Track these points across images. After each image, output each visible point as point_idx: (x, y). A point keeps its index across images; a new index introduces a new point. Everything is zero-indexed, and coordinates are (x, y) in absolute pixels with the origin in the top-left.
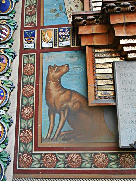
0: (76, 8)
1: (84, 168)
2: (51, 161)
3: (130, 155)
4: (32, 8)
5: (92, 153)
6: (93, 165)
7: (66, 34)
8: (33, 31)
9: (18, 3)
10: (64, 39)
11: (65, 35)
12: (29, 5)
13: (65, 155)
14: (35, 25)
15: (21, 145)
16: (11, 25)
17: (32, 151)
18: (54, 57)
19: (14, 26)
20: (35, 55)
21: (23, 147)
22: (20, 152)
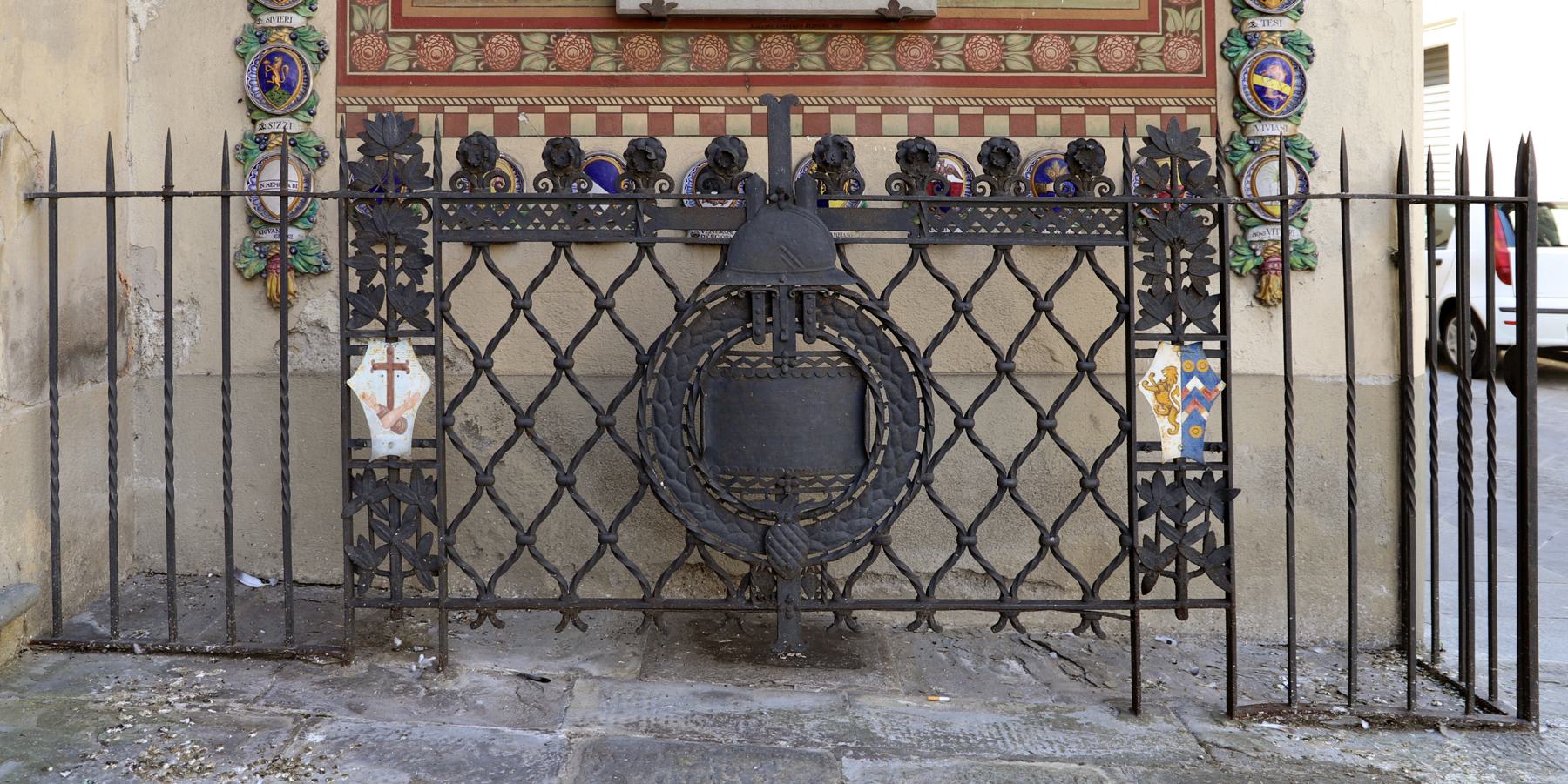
1: (525, 70)
2: (439, 54)
3: (651, 39)
5: (549, 34)
6: (551, 64)
13: (477, 38)
15: (355, 12)
17: (386, 28)
21: (362, 18)
22: (352, 29)
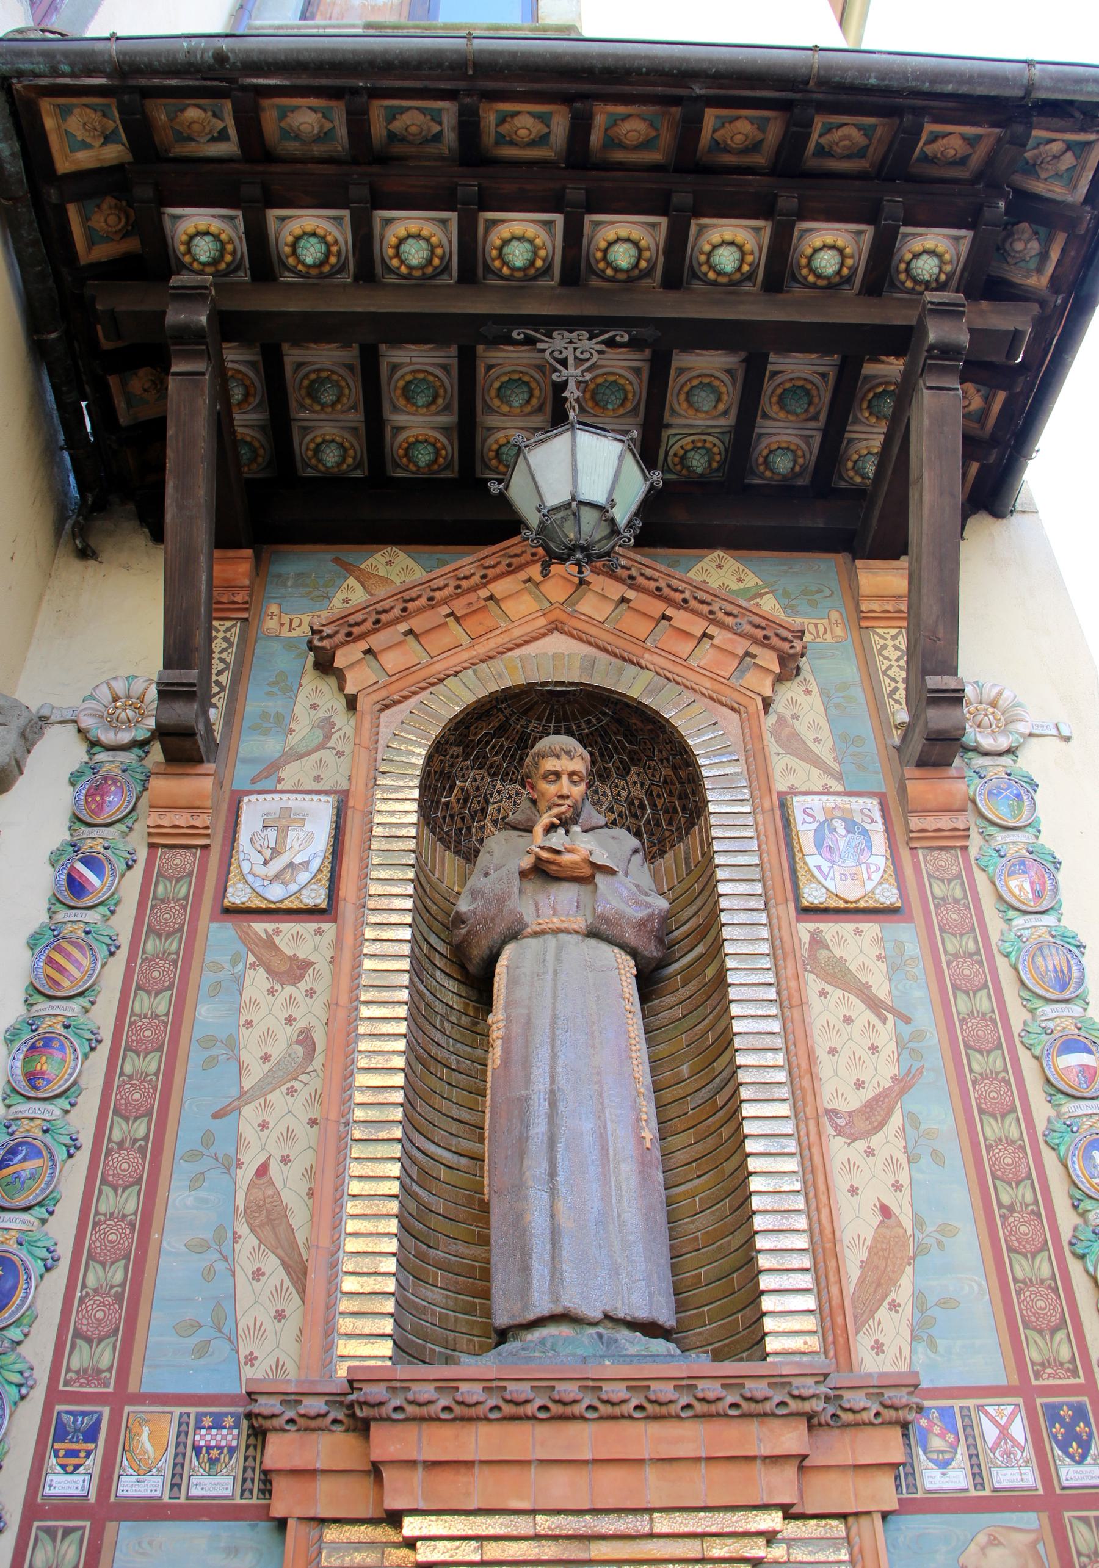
0: (279, 1325)
4: (105, 1306)
7: (223, 1443)
8: (95, 1416)
9: (54, 1273)
10: (213, 1462)
11: (220, 1448)
12: (95, 1291)
14: (106, 1385)
16: (10, 1383)
18: (160, 1547)
19: (19, 1386)
20: (84, 1528)
